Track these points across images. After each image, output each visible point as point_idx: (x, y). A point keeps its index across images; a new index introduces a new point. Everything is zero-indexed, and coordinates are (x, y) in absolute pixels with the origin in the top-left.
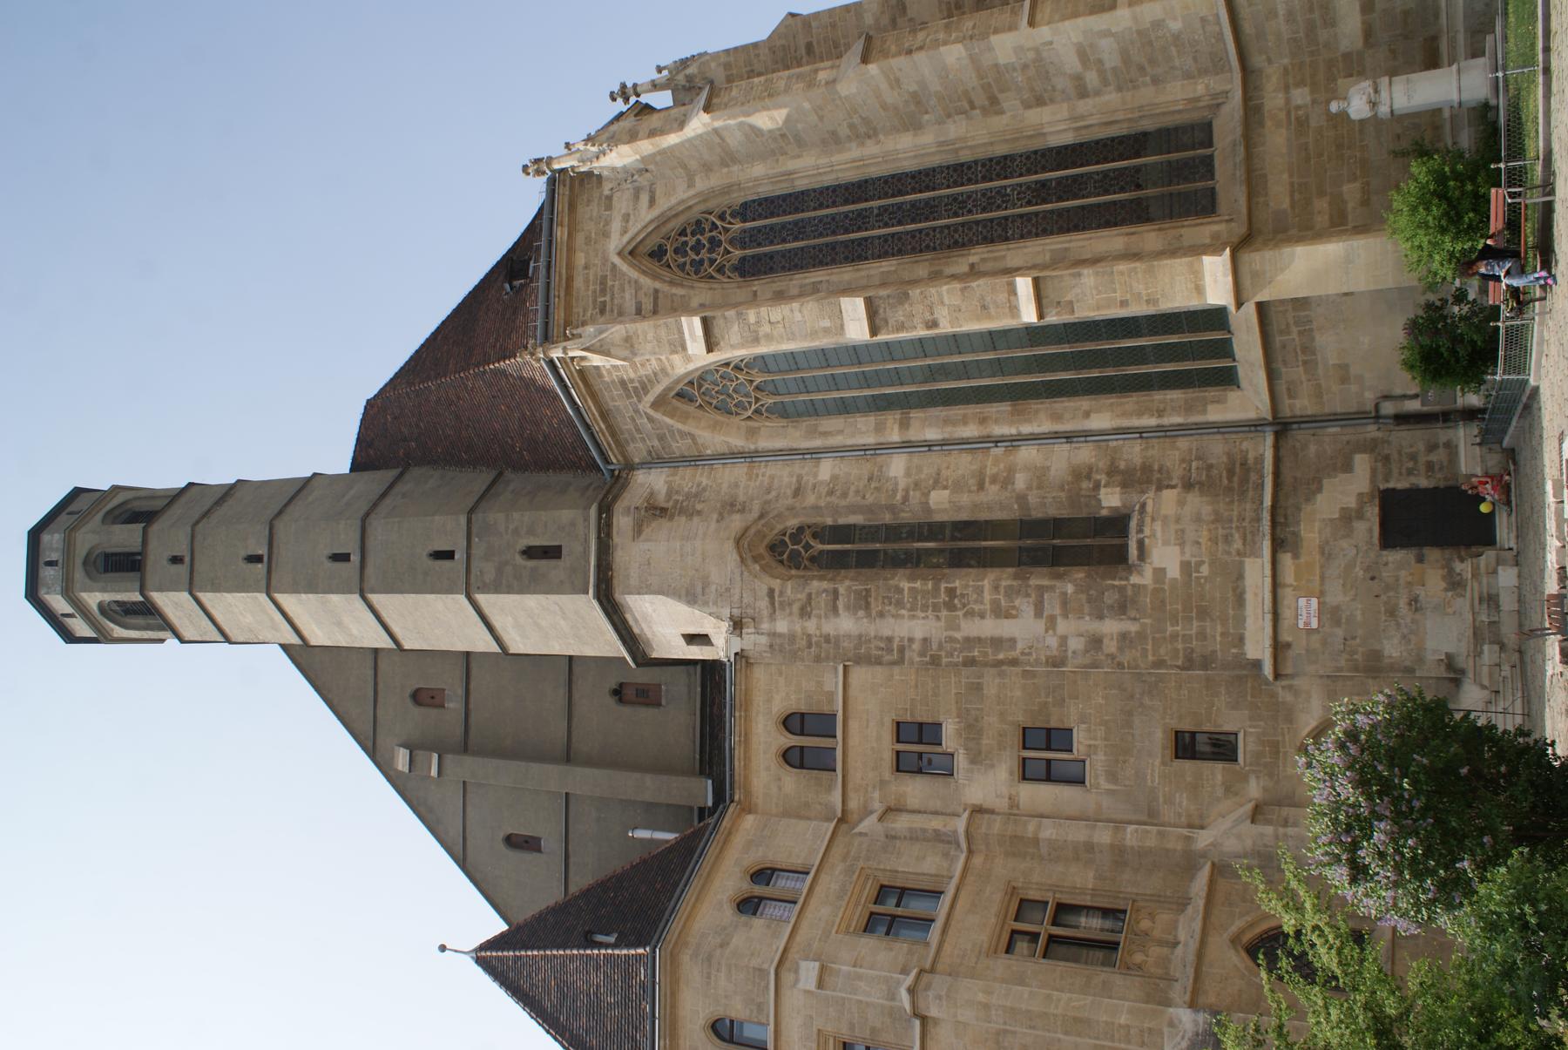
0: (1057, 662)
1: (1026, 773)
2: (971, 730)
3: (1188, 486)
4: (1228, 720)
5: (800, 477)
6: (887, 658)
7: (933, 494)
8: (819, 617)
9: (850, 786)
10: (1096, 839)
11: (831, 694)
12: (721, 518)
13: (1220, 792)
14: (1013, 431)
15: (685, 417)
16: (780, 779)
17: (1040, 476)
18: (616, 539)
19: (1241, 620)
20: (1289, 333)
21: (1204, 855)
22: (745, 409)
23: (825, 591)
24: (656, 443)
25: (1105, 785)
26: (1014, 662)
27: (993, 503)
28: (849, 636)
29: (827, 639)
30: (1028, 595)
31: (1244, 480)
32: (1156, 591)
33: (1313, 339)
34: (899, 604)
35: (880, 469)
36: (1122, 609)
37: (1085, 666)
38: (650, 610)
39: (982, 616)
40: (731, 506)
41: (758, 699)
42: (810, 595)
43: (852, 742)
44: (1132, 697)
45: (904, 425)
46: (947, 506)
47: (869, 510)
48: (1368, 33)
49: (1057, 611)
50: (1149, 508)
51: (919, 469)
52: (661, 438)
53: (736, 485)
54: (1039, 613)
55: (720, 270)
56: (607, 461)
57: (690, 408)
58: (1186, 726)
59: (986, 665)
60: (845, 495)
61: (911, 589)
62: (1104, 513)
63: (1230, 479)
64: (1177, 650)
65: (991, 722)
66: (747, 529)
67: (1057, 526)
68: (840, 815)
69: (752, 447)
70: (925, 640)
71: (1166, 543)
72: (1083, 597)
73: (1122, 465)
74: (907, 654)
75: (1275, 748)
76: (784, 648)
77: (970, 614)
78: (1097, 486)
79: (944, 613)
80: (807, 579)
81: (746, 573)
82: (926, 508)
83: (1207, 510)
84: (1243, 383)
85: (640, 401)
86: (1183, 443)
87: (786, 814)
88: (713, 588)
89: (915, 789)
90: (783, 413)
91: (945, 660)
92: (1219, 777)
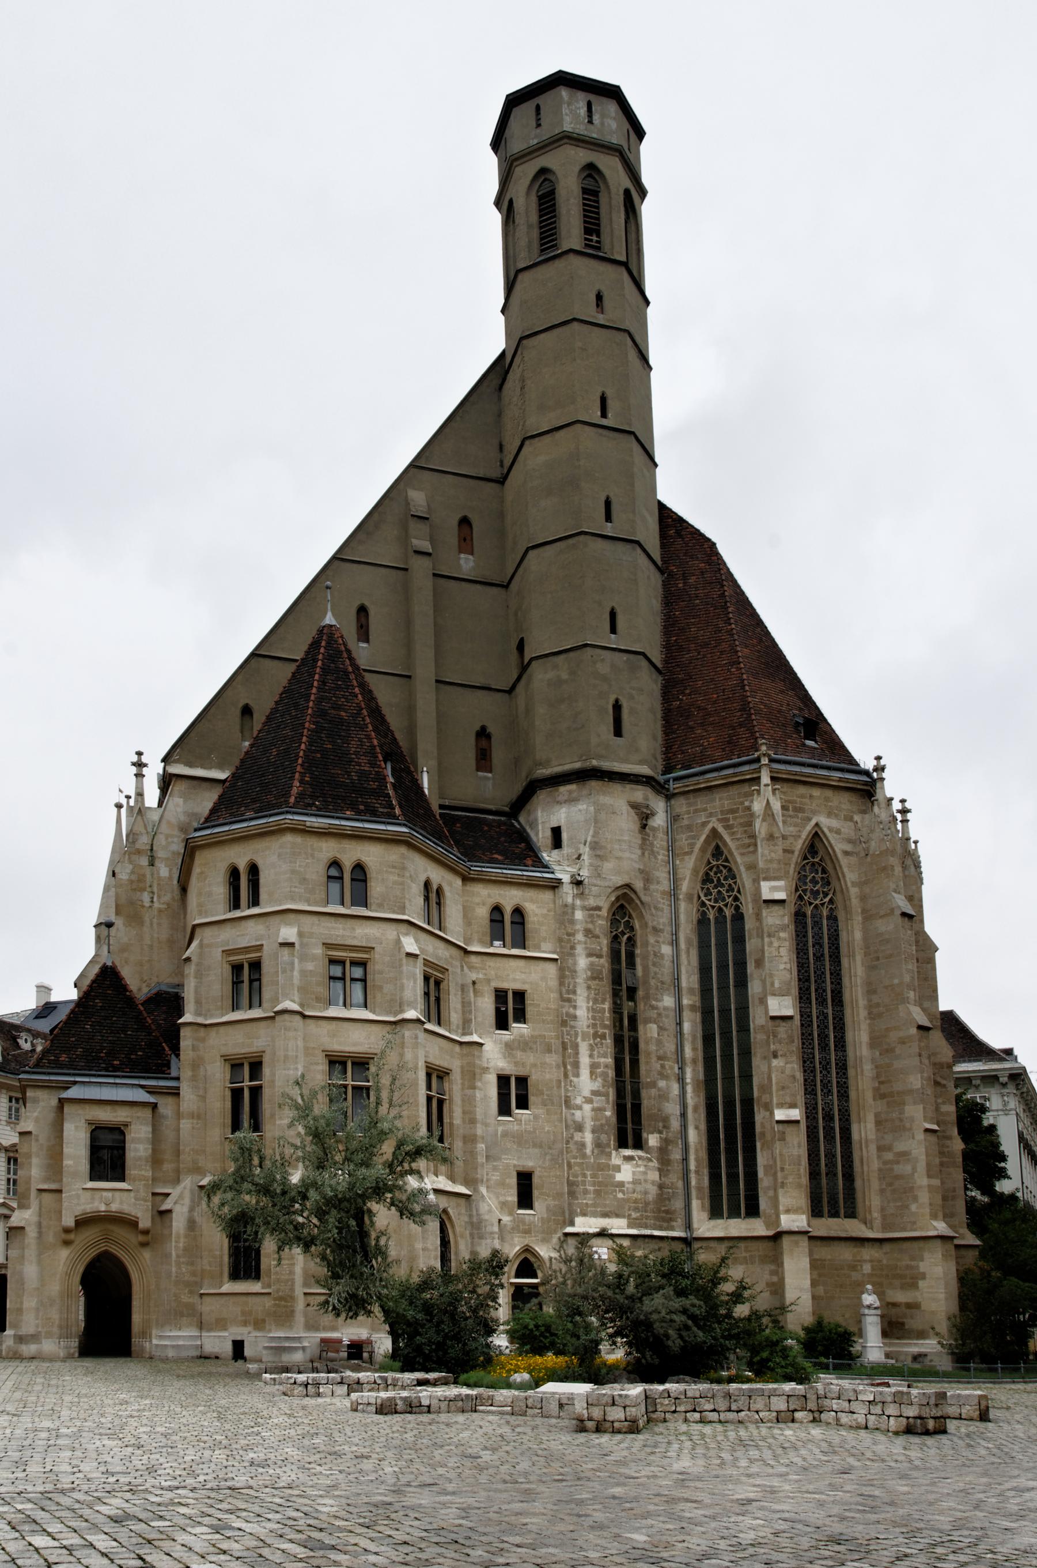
0: (567, 1102)
1: (503, 1080)
2: (524, 1044)
3: (661, 1187)
4: (540, 1204)
5: (662, 931)
6: (564, 990)
7: (654, 1027)
8: (585, 943)
9: (485, 958)
10: (478, 1125)
11: (538, 948)
12: (641, 871)
13: (502, 1199)
14: (688, 1080)
15: (703, 850)
16: (484, 904)
17: (664, 1096)
18: (629, 786)
19: (595, 1215)
20: (746, 1251)
21: (476, 1190)
22: (706, 895)
23: (601, 949)
24: (686, 822)
25: (500, 1129)
26: (566, 1076)
27: (649, 1067)
28: (575, 964)
29: (573, 948)
30: (603, 1086)
31: (664, 1220)
32: (609, 1165)
33: (741, 1264)
34: (595, 1001)
35: (668, 989)
36: (598, 1144)
37: (566, 1121)
38: (580, 807)
39: (591, 1056)
40: (648, 880)
41: (531, 893)
42: (598, 937)
43: (513, 963)
44: (550, 1148)
45: (692, 1008)
46: (649, 1035)
47: (646, 982)
48: (894, 1305)
49: (595, 1105)
50: (650, 1164)
51: (667, 1016)
52: (689, 828)
53: (658, 883)
54: (595, 1093)
55: (800, 898)
56: (676, 779)
57: (708, 855)
58: (536, 1180)
59: (564, 1056)
60: (654, 964)
61: (604, 1009)
62: (644, 1135)
63: (664, 1211)
64: (576, 1176)
65: (530, 1058)
66: (635, 892)
67: (637, 1108)
68: (469, 949)
69: (681, 897)
70: (575, 1017)
71: (634, 1173)
72: (604, 1122)
73: (670, 1148)
74: (566, 1004)
75: (527, 1232)
76: (565, 914)
77: (592, 1048)
78: (660, 1132)
79: (592, 1031)
80: (606, 935)
81: (610, 890)
82: (647, 1021)
83: (651, 1197)
84: (713, 1222)
85: (718, 820)
86: (680, 1184)
87: (464, 907)
88: (599, 863)
89: (487, 1005)
90: (702, 922)
91: (564, 1029)
92: (510, 1199)
